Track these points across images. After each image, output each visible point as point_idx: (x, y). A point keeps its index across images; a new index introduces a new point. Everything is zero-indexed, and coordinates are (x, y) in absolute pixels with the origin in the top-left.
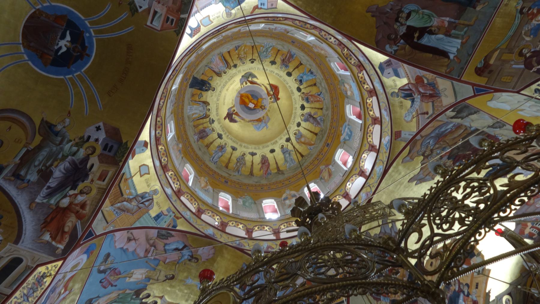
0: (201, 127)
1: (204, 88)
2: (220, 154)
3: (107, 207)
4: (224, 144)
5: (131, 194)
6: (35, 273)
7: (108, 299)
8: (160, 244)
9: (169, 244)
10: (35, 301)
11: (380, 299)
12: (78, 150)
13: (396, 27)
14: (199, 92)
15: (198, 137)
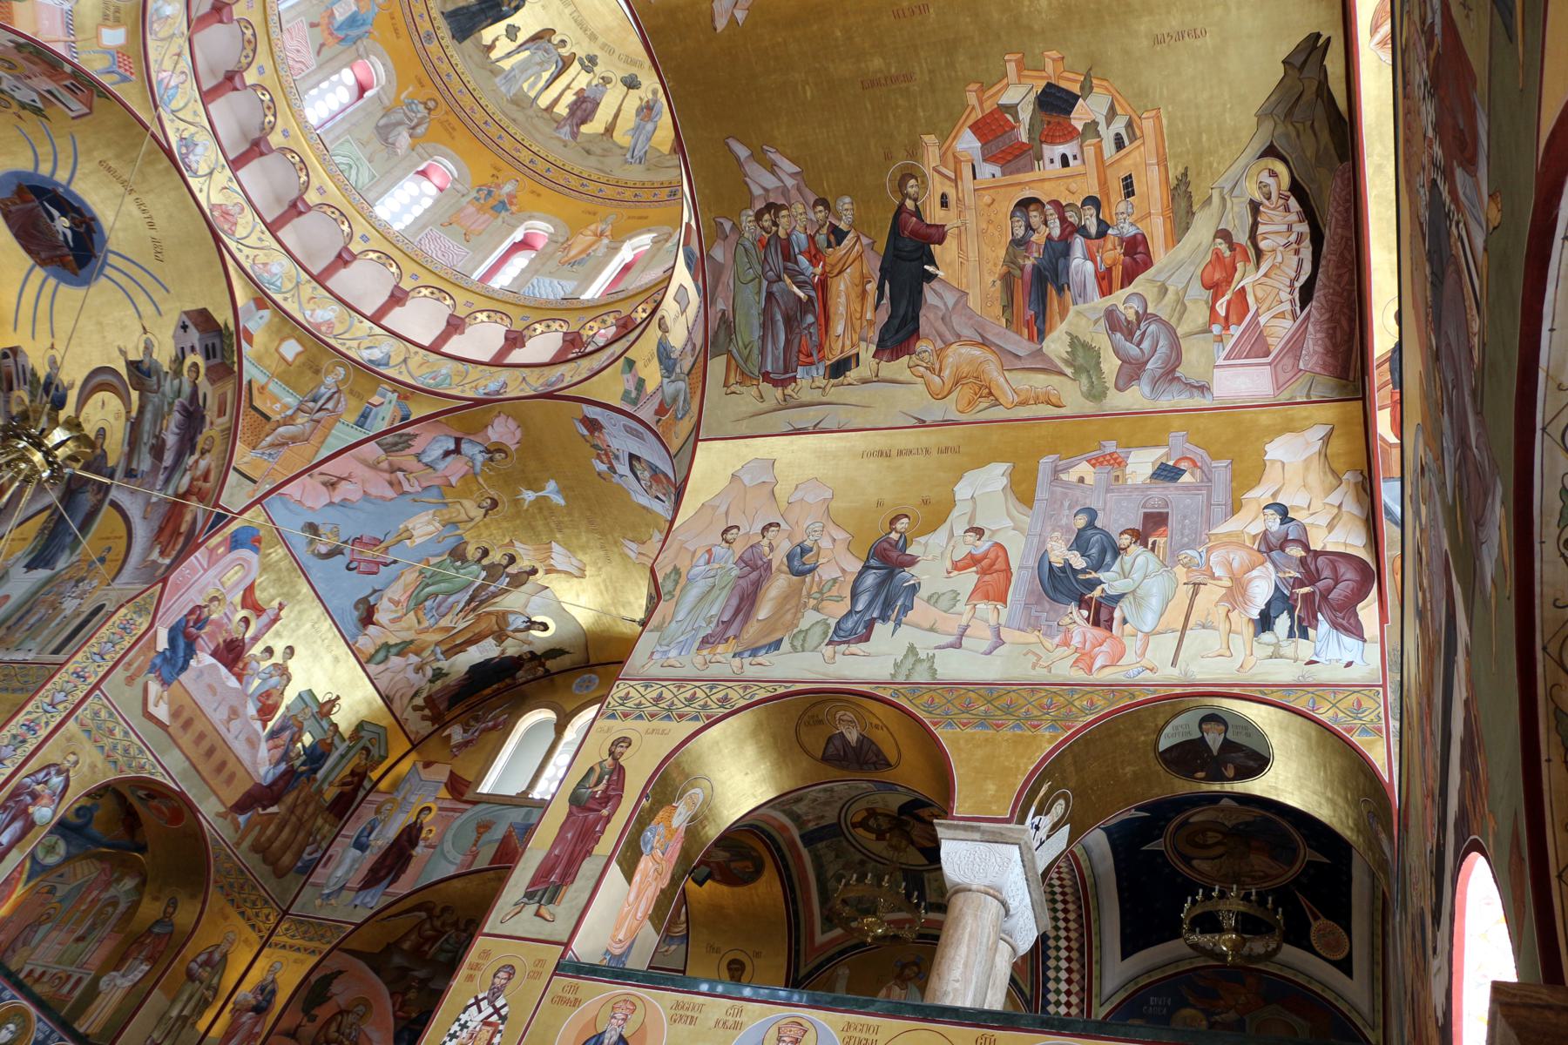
0: (569, 98)
1: (505, 8)
2: (650, 126)
3: (243, 456)
4: (650, 96)
5: (287, 407)
6: (115, 618)
7: (406, 586)
8: (405, 459)
9: (424, 452)
10: (118, 656)
11: (794, 379)
12: (181, 382)
14: (500, 27)
15: (571, 126)
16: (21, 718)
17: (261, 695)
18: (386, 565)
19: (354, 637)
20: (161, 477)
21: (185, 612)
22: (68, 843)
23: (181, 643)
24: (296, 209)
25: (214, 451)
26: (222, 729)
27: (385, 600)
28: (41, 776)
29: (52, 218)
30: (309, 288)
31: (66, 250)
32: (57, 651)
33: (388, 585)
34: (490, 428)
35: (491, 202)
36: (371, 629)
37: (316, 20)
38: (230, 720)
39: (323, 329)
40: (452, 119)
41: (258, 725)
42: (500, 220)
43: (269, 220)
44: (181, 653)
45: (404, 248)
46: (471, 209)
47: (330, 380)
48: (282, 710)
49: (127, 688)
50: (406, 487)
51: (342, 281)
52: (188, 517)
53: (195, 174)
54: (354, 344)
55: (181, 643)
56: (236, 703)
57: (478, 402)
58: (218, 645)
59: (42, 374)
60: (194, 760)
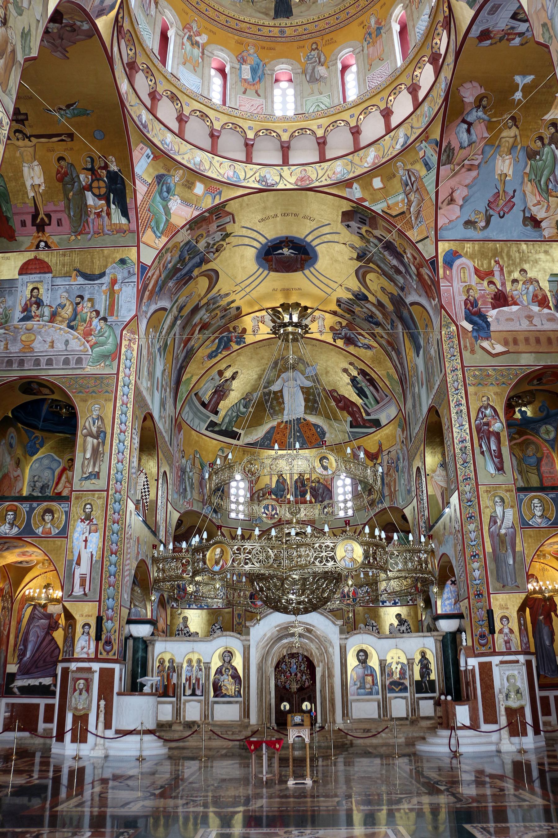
3: (413, 235)
7: (532, 193)
8: (459, 155)
9: (461, 143)
13: (55, 31)
16: (452, 405)
17: (533, 299)
18: (513, 197)
19: (541, 235)
20: (408, 277)
21: (463, 307)
22: (550, 424)
23: (476, 319)
24: (322, 143)
25: (406, 246)
26: (533, 328)
27: (532, 208)
28: (480, 415)
29: (283, 254)
30: (356, 158)
31: (299, 256)
32: (441, 372)
33: (525, 202)
34: (465, 99)
35: (374, 36)
36: (543, 224)
37: (244, 90)
38: (531, 322)
39: (376, 161)
40: (326, 37)
41: (546, 311)
42: (384, 35)
43: (318, 160)
44: (481, 322)
45: (367, 97)
46: (371, 49)
47: (401, 172)
48: (549, 294)
49: (475, 355)
50: (476, 163)
51: (365, 138)
52: (426, 277)
53: (277, 184)
54: (391, 149)
55: (476, 319)
56: (526, 314)
57: (446, 99)
58: (491, 303)
59: (351, 297)
60: (535, 351)
